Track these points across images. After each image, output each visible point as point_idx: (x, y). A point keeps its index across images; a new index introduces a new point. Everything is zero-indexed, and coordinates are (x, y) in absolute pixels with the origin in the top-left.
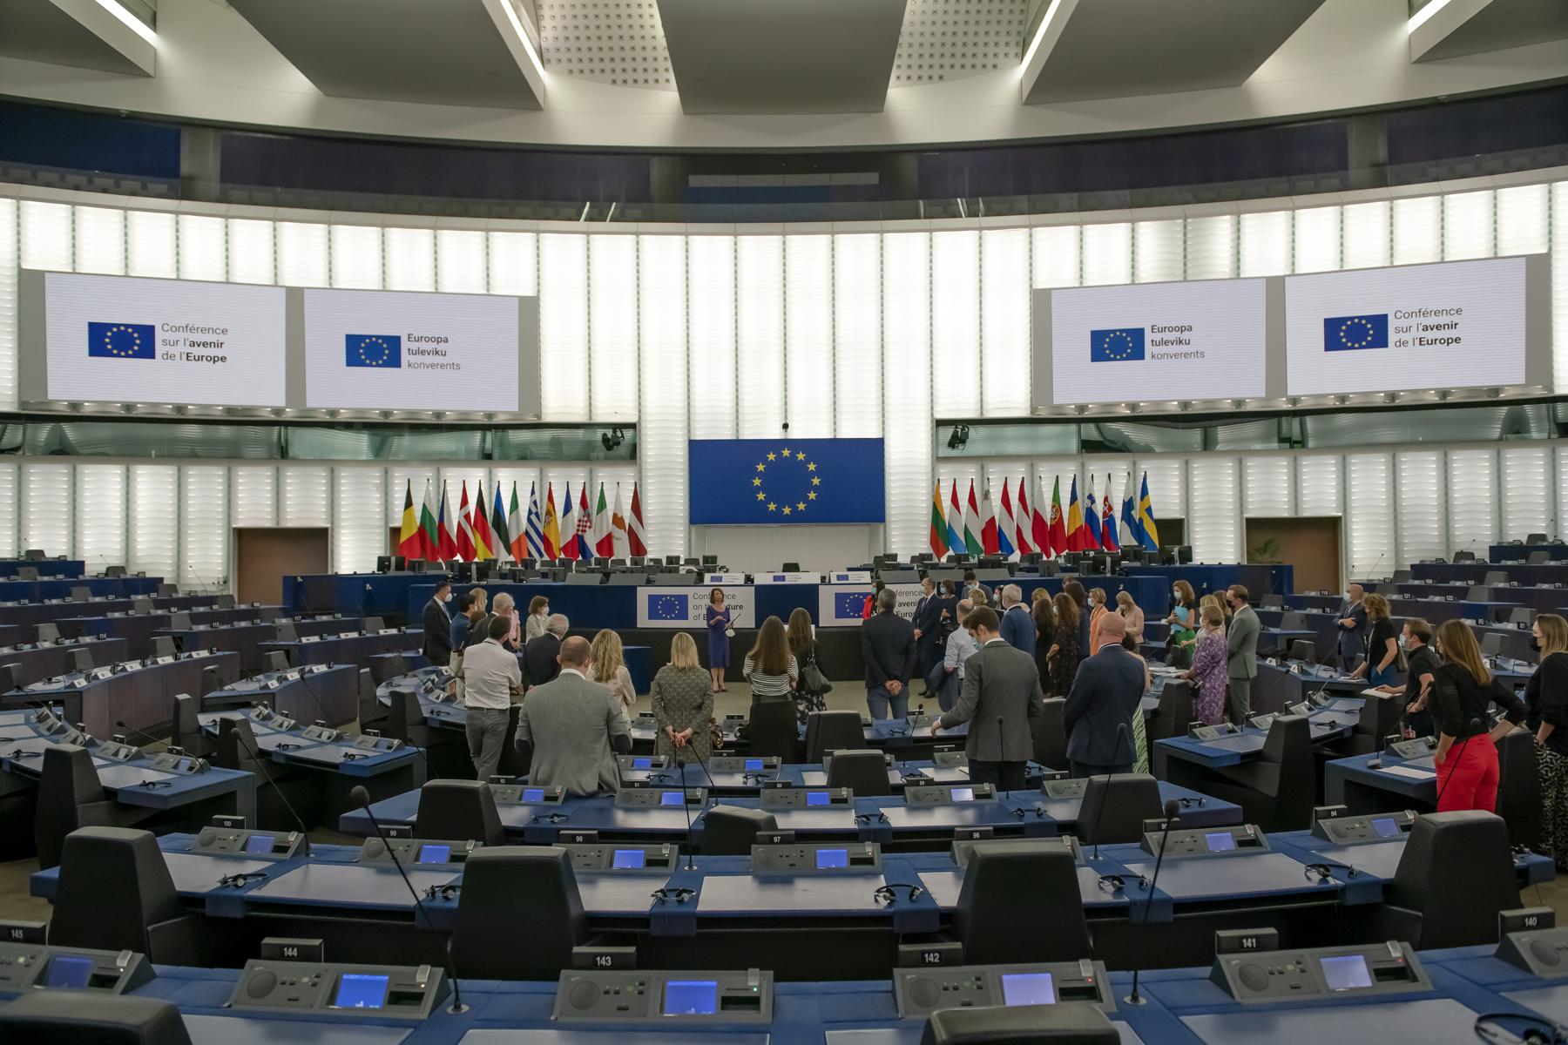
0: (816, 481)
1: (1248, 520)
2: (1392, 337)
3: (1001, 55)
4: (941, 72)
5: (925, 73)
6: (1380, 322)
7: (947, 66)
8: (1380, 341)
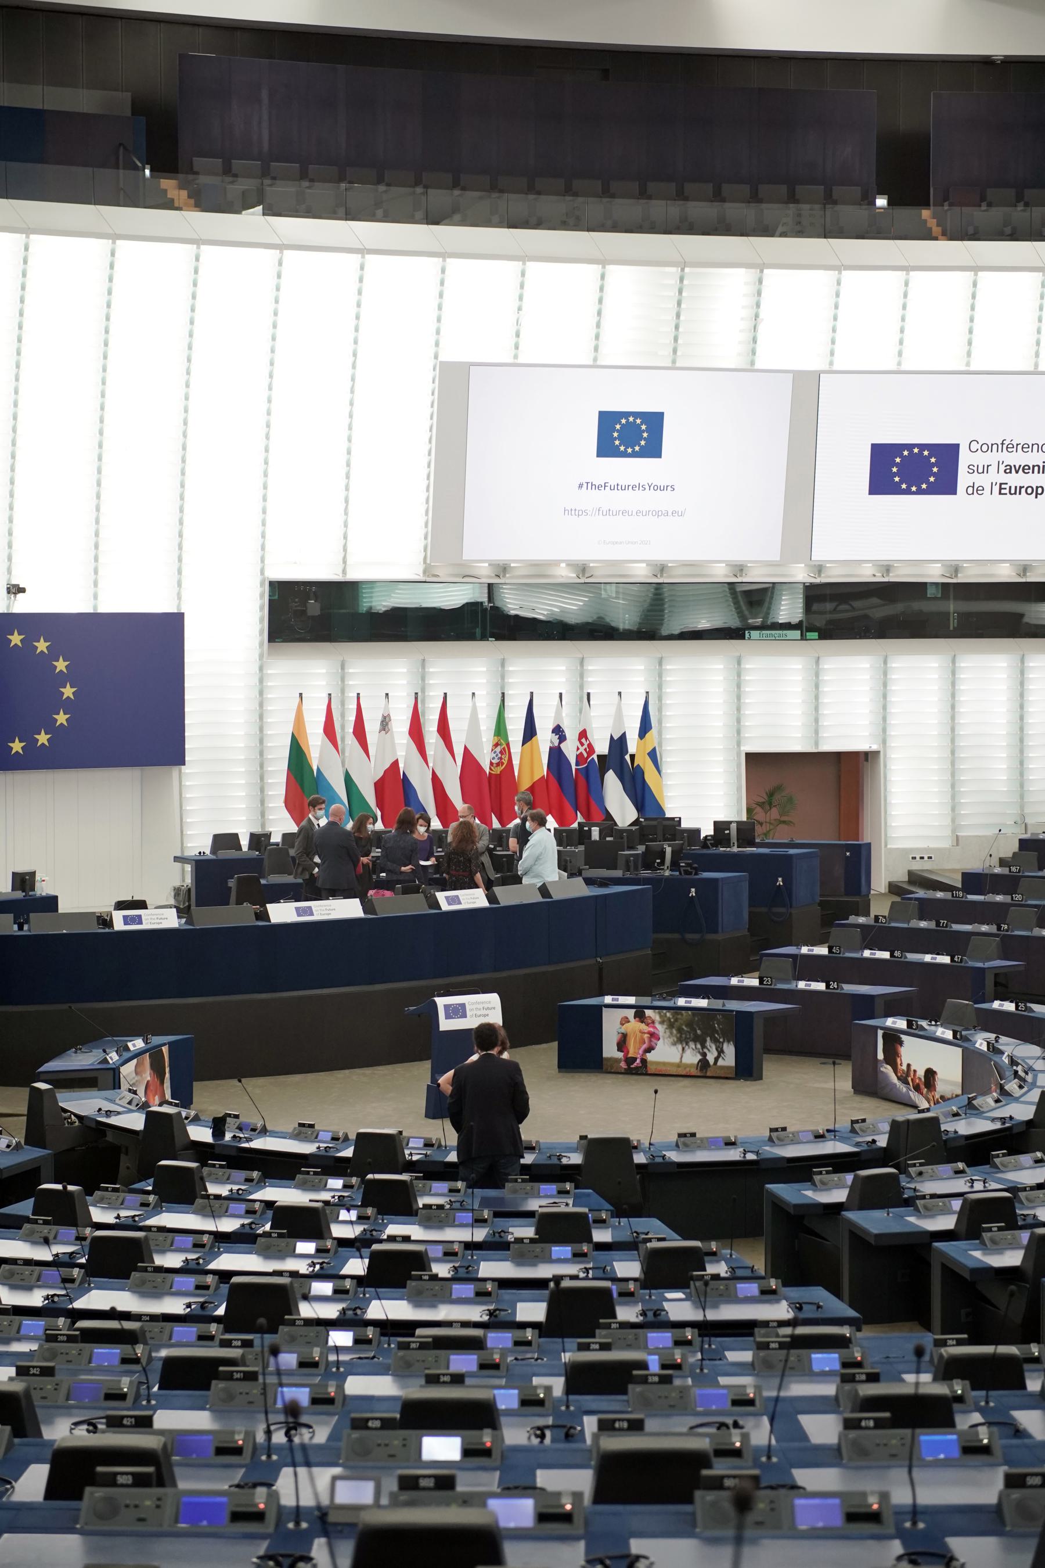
0: (68, 692)
1: (749, 756)
2: (964, 479)
6: (948, 454)
8: (947, 485)
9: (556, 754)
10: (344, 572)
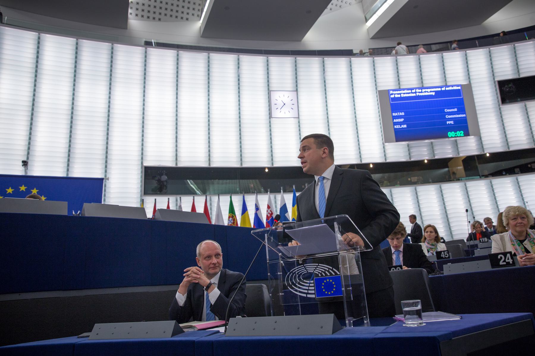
3: (190, 14)
4: (160, 17)
5: (151, 15)
7: (163, 14)
9: (257, 219)
10: (176, 164)
